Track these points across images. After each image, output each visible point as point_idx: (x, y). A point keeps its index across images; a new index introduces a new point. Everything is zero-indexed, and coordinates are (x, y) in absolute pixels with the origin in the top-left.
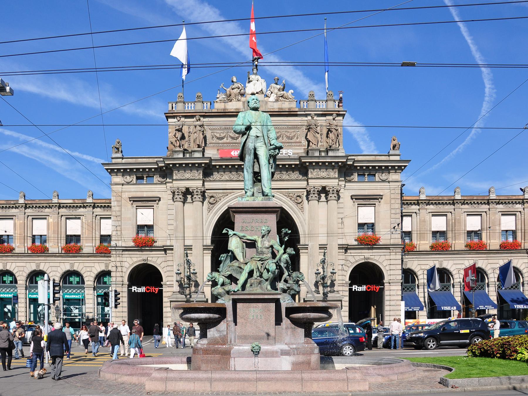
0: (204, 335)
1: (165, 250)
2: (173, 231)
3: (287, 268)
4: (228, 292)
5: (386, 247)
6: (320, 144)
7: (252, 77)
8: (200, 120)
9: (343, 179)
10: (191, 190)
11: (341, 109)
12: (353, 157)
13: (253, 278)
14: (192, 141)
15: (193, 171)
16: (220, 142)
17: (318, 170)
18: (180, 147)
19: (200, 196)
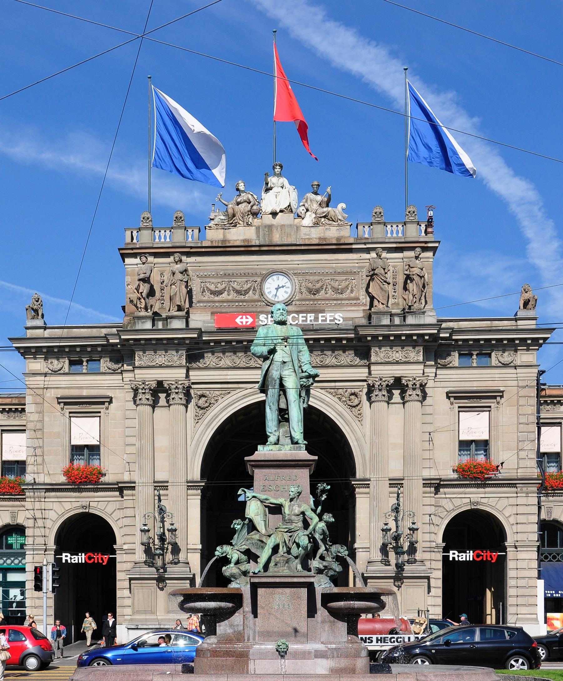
0: (212, 631)
1: (121, 488)
2: (133, 456)
3: (324, 540)
4: (245, 573)
5: (510, 483)
6: (391, 301)
7: (273, 180)
8: (181, 261)
9: (433, 363)
10: (166, 385)
11: (430, 237)
12: (451, 325)
13: (279, 555)
14: (167, 298)
15: (169, 352)
16: (216, 298)
17: (388, 348)
18: (146, 309)
19: (181, 396)
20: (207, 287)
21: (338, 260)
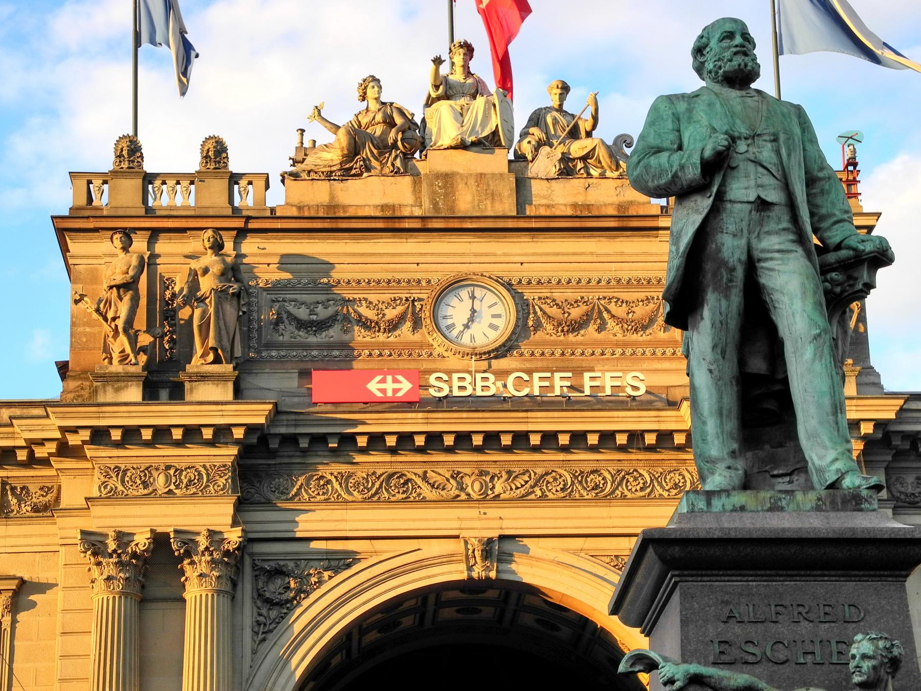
16: (313, 339)
20: (289, 314)
21: (622, 254)
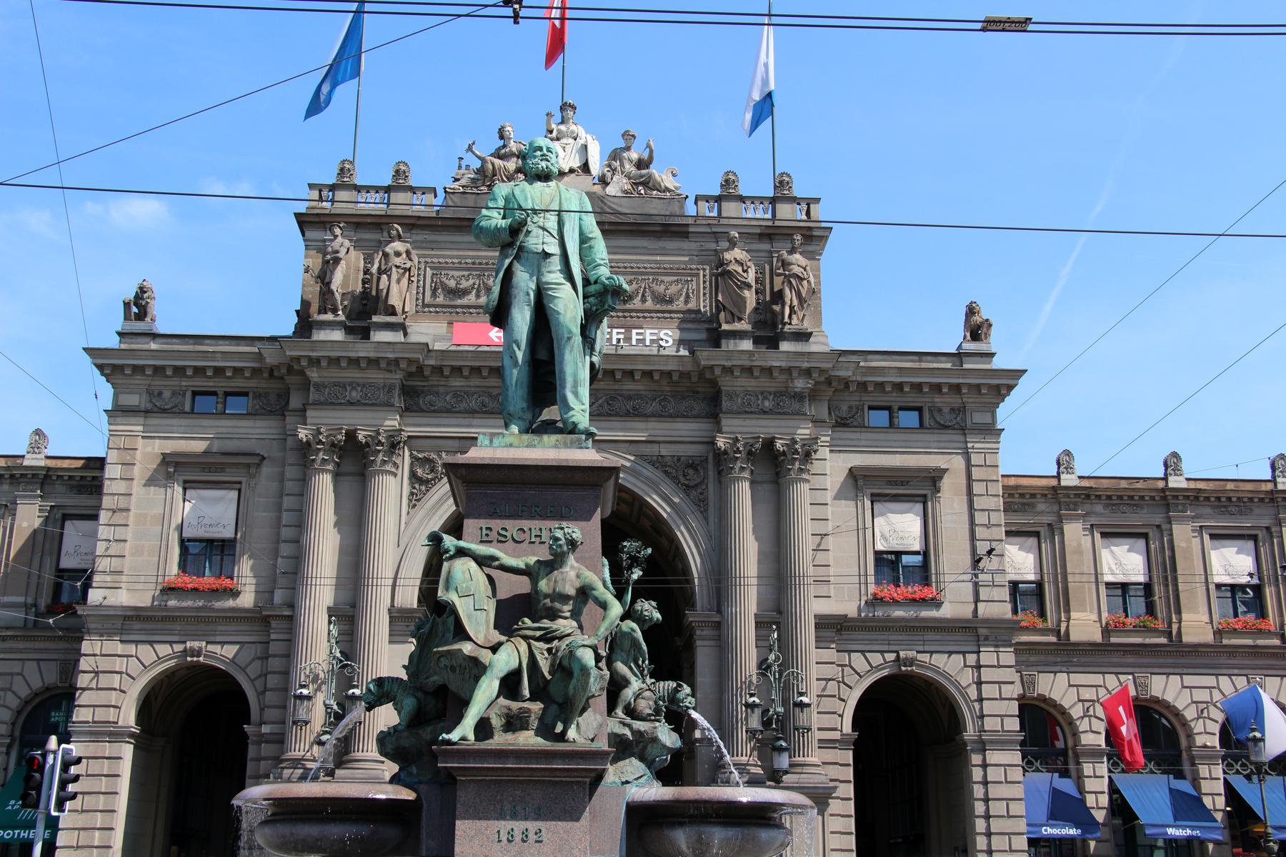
16: (459, 302)
